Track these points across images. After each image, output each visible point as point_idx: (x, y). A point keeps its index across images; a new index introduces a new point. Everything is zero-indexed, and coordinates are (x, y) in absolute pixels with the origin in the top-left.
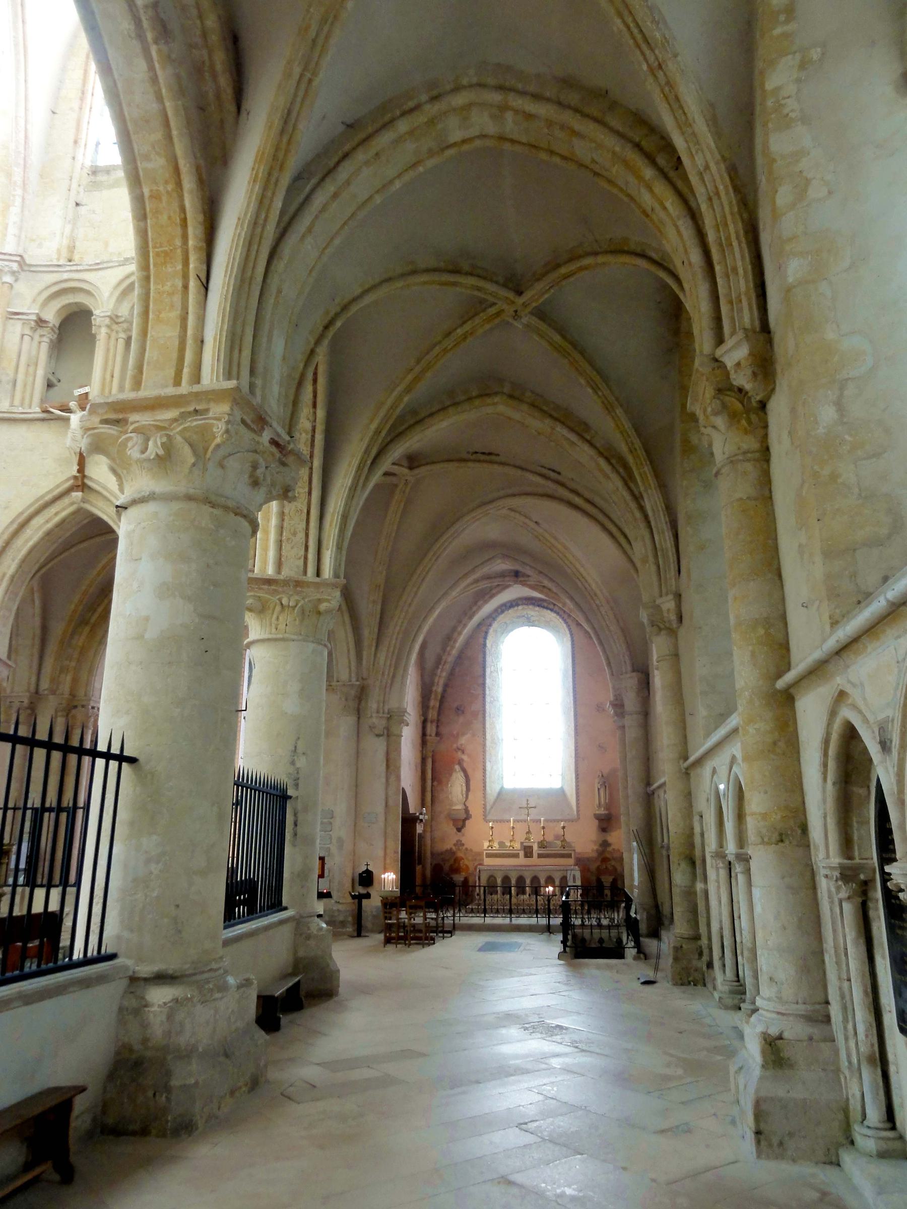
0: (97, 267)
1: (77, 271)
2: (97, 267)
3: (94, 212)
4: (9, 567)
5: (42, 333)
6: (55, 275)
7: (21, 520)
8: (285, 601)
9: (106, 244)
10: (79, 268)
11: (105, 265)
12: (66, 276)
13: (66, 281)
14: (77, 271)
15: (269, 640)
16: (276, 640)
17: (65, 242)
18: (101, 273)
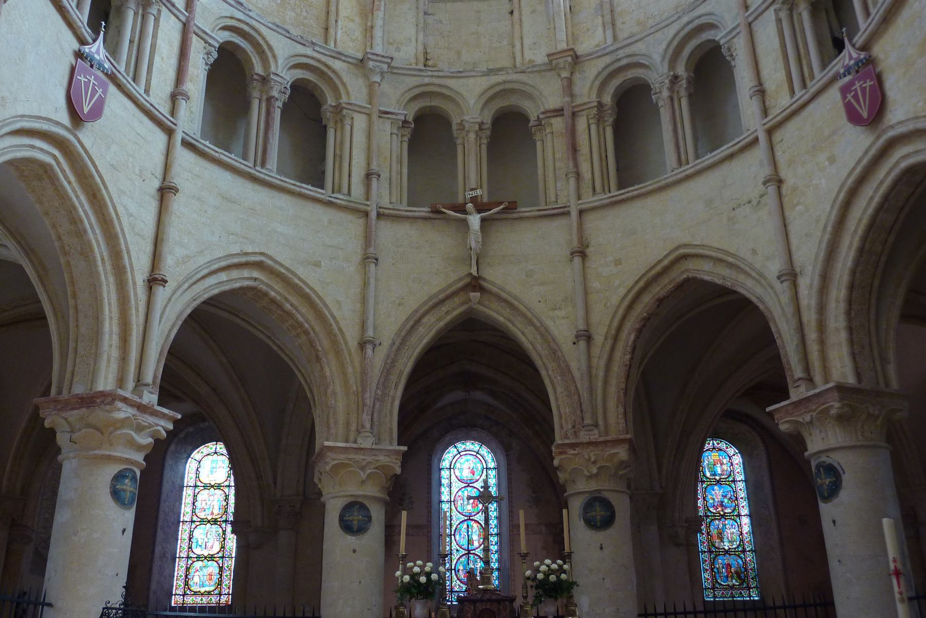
0: (458, 75)
1: (438, 77)
2: (458, 75)
3: (441, 21)
4: (406, 365)
5: (404, 134)
6: (416, 78)
7: (416, 318)
8: (871, 410)
9: (459, 53)
10: (440, 74)
11: (467, 74)
12: (427, 80)
13: (427, 85)
14: (438, 77)
15: (861, 447)
16: (861, 447)
17: (421, 48)
18: (462, 80)
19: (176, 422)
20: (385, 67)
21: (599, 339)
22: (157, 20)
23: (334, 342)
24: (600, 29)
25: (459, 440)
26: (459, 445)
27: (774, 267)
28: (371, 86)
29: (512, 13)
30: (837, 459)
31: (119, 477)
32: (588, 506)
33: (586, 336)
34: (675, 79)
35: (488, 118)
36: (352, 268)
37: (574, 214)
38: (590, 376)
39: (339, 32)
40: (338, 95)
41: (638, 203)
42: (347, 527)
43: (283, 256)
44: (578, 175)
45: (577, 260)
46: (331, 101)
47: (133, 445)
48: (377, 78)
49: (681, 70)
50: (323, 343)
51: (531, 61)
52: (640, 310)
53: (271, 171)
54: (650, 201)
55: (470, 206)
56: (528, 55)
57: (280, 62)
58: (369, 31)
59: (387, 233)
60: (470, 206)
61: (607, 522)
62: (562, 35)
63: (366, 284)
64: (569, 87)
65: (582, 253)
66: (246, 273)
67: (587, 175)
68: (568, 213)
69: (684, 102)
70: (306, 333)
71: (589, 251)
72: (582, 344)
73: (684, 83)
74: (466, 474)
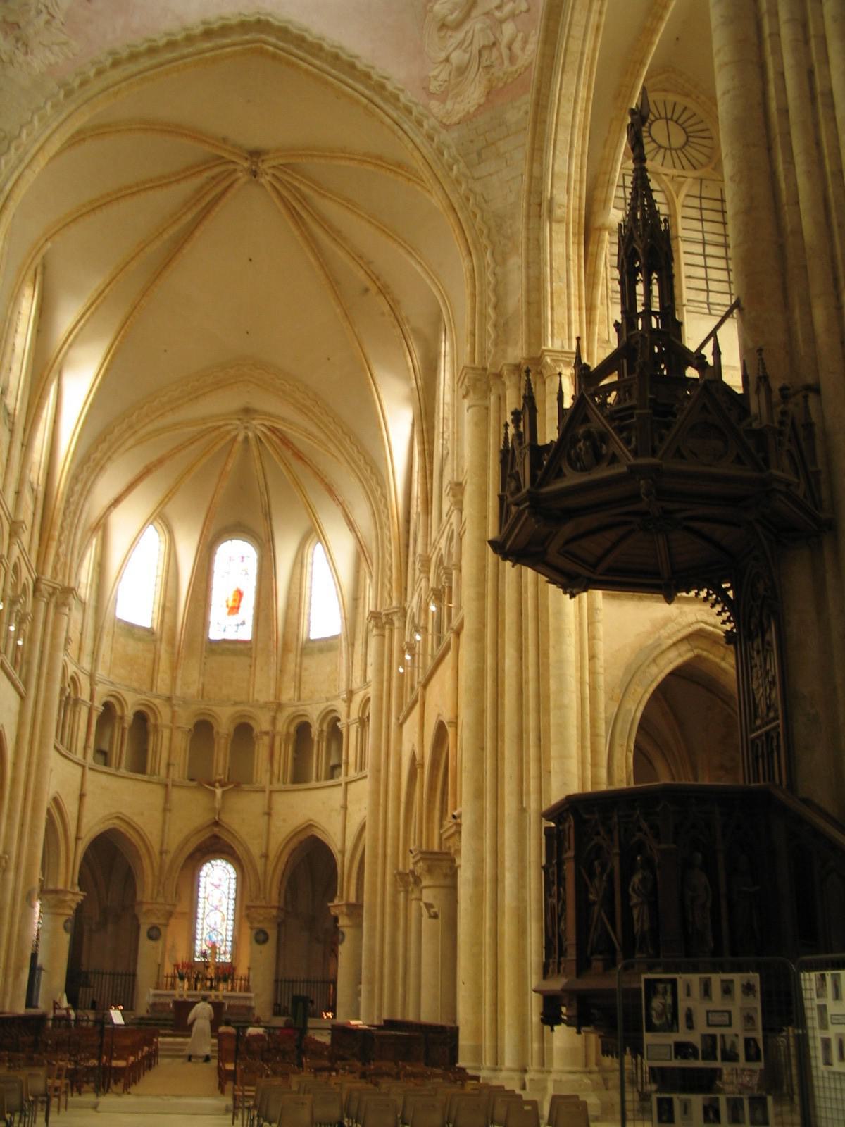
12: (202, 707)
17: (201, 687)
19: (84, 896)
20: (181, 703)
21: (272, 855)
22: (80, 713)
23: (148, 850)
24: (293, 690)
25: (213, 859)
26: (213, 862)
27: (339, 844)
28: (173, 712)
29: (251, 666)
30: (346, 931)
31: (66, 921)
32: (257, 934)
33: (266, 856)
34: (321, 732)
35: (232, 730)
36: (158, 815)
37: (267, 792)
38: (265, 873)
39: (159, 681)
40: (156, 719)
41: (297, 794)
42: (151, 937)
43: (127, 812)
44: (272, 773)
45: (266, 817)
46: (152, 720)
47: (71, 907)
48: (176, 709)
49: (325, 727)
50: (143, 851)
51: (257, 701)
52: (292, 845)
53: (123, 771)
54: (302, 794)
55: (217, 785)
56: (256, 696)
57: (129, 707)
58: (174, 679)
59: (176, 794)
60: (217, 785)
61: (265, 941)
62: (272, 691)
63: (164, 822)
64: (274, 721)
65: (269, 814)
66: (111, 822)
67: (276, 771)
68: (264, 791)
69: (324, 744)
70: (135, 846)
71: (272, 812)
72: (263, 860)
73: (325, 734)
74: (217, 882)
